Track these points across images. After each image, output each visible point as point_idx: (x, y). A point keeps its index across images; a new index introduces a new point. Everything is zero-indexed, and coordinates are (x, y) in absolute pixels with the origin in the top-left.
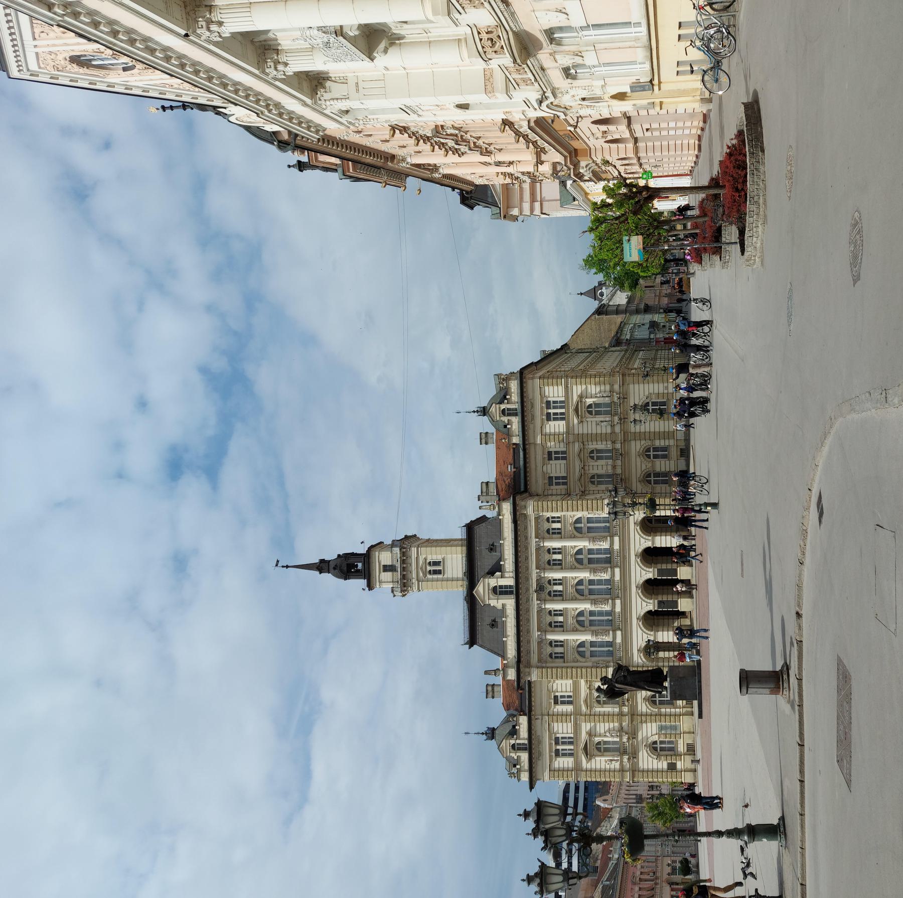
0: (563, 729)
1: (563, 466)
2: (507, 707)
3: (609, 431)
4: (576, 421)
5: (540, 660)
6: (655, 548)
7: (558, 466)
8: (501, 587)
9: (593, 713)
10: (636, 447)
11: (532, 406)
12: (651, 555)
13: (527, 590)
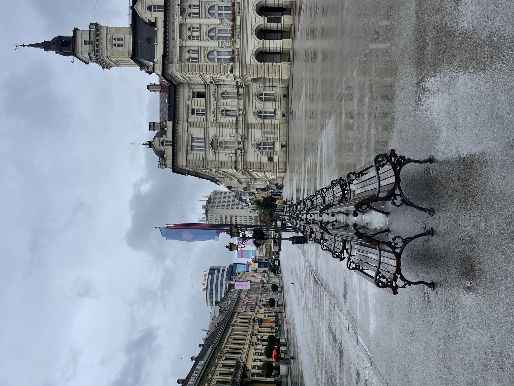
0: (198, 133)
8: (155, 6)
13: (174, 8)
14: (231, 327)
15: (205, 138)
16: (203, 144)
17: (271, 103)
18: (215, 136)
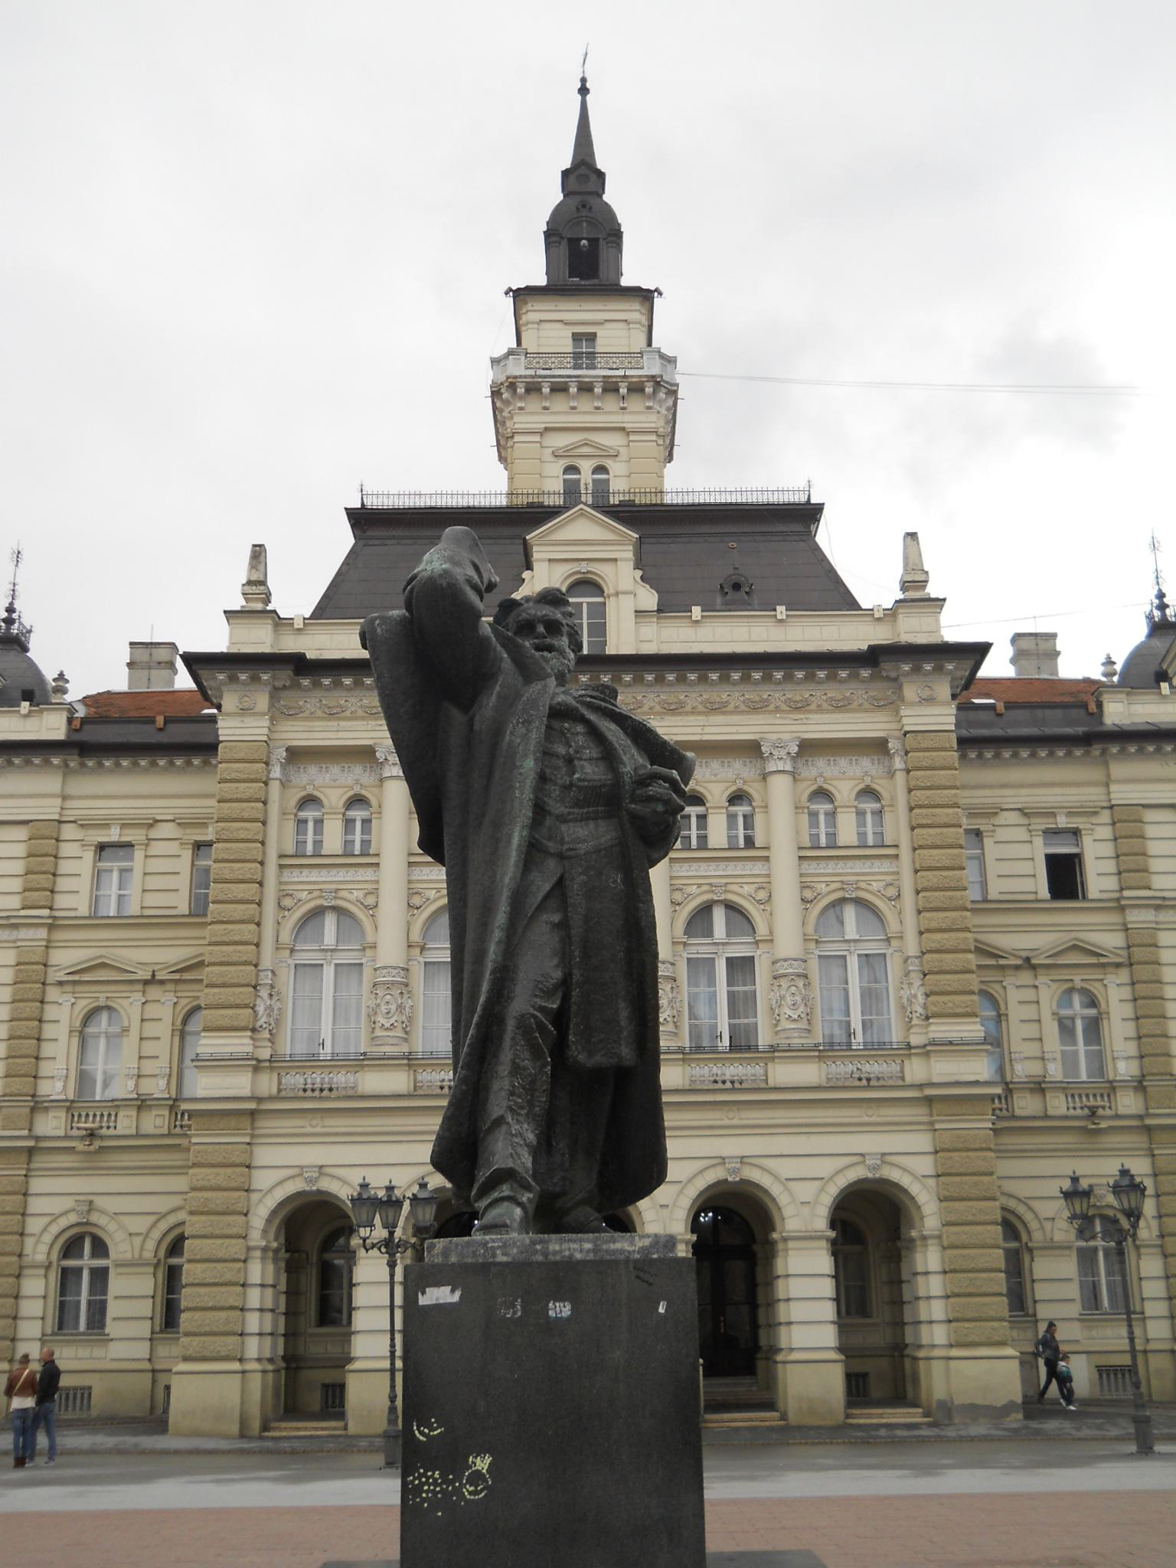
1: (1027, 885)
5: (296, 755)
6: (770, 1251)
7: (1025, 868)
9: (52, 993)
17: (145, 1308)
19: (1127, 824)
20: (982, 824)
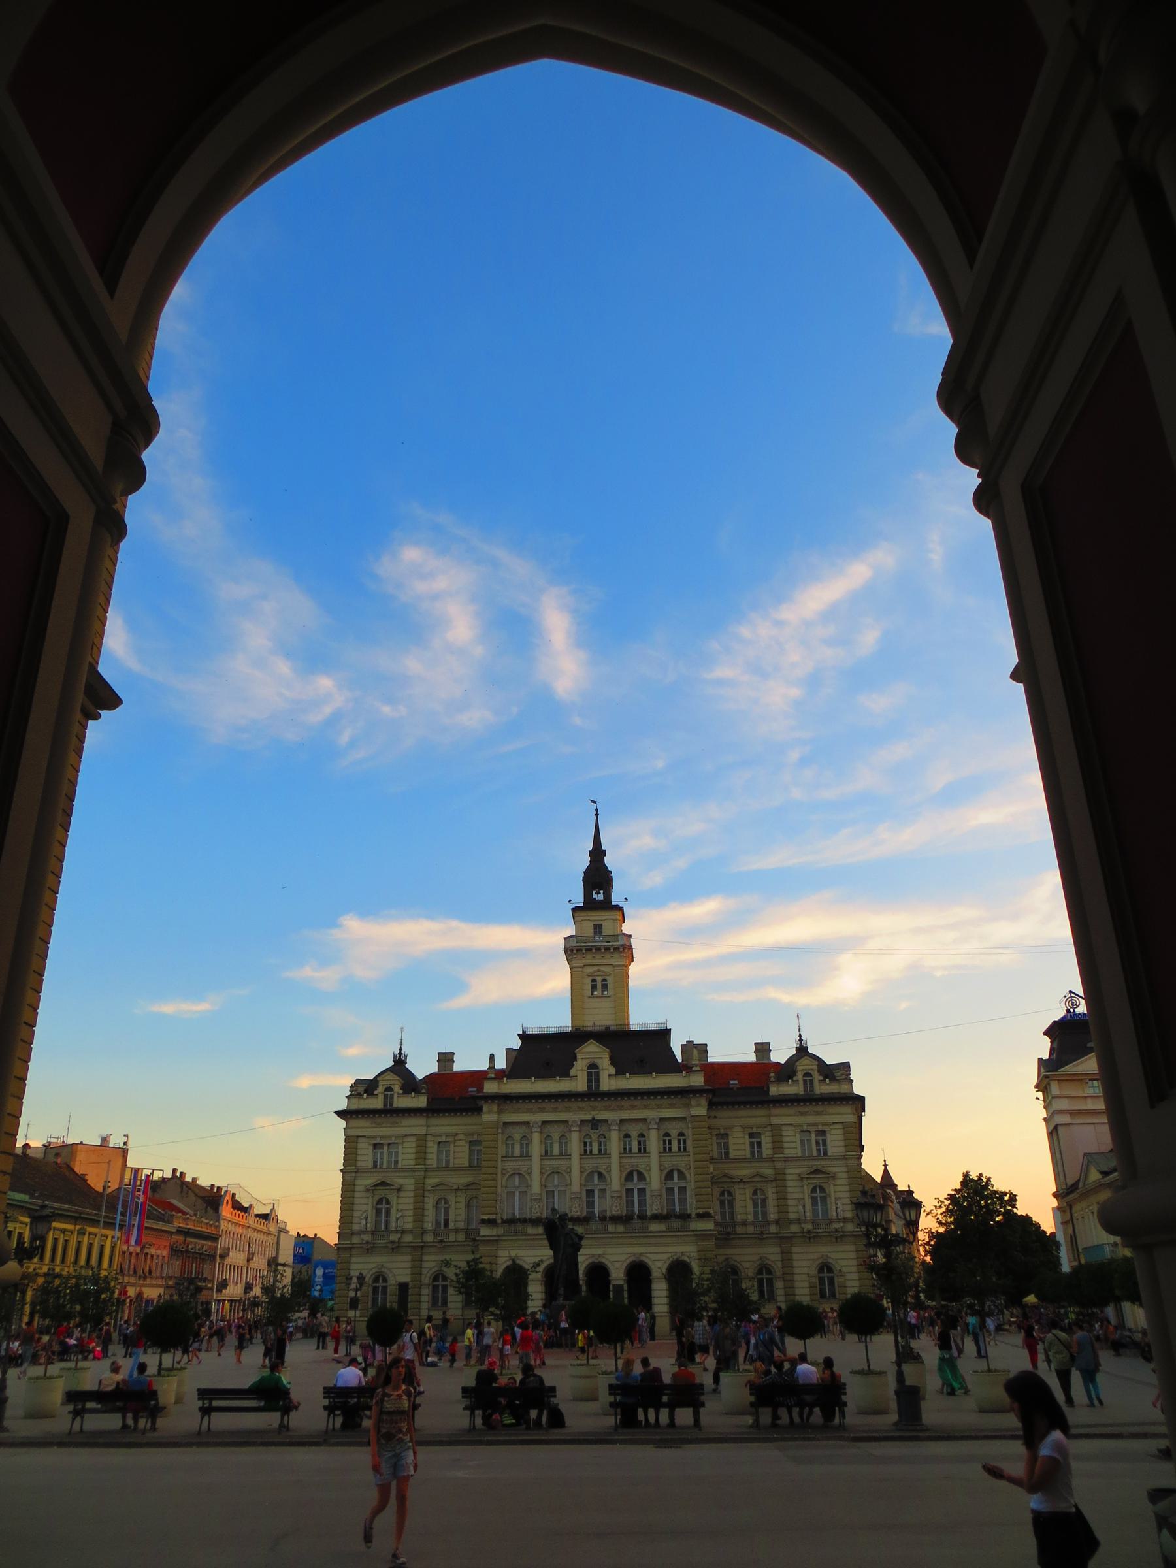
2: (430, 1078)
3: (792, 1216)
4: (798, 1171)
5: (505, 1124)
8: (597, 1074)
9: (427, 1194)
10: (772, 1254)
11: (818, 1113)
12: (639, 1273)
13: (594, 1109)
14: (78, 1227)
15: (397, 1169)
16: (385, 1166)
18: (399, 1190)
19: (776, 1130)
20: (728, 1131)
